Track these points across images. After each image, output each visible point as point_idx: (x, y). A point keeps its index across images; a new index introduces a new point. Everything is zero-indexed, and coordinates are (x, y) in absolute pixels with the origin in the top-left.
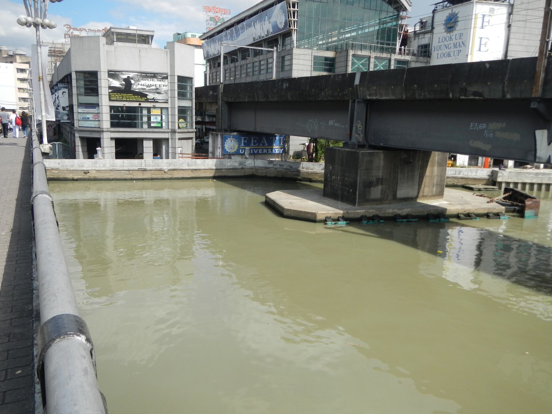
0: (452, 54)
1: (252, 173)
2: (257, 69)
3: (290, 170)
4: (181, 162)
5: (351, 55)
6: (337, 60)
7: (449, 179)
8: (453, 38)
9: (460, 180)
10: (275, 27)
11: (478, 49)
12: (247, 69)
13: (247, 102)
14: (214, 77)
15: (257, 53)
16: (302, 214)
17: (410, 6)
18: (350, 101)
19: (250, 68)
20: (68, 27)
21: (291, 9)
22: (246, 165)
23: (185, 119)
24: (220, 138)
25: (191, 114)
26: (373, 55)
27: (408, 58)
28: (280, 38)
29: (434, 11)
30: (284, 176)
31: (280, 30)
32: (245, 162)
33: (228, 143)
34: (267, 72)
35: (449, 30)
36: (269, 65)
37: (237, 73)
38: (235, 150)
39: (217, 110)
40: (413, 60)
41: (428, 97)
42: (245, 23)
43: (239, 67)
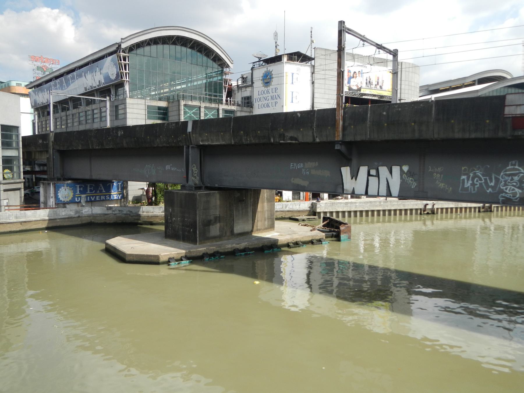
0: (270, 105)
1: (89, 221)
2: (90, 117)
3: (130, 215)
4: (7, 215)
5: (183, 105)
6: (170, 110)
7: (278, 212)
8: (270, 91)
9: (287, 213)
10: (107, 78)
12: (79, 118)
13: (81, 150)
14: (44, 126)
15: (89, 103)
16: (145, 258)
17: (232, 63)
18: (185, 147)
19: (82, 117)
21: (122, 61)
22: (82, 213)
23: (11, 169)
24: (52, 187)
25: (17, 164)
26: (203, 105)
27: (233, 108)
28: (112, 88)
29: (252, 69)
30: (124, 221)
31: (112, 81)
32: (82, 210)
33: (62, 192)
34: (101, 121)
35: (266, 85)
36: (102, 114)
37: (69, 121)
38: (70, 198)
39: (48, 159)
40: (238, 110)
41: (253, 142)
42: (75, 73)
43: (71, 116)
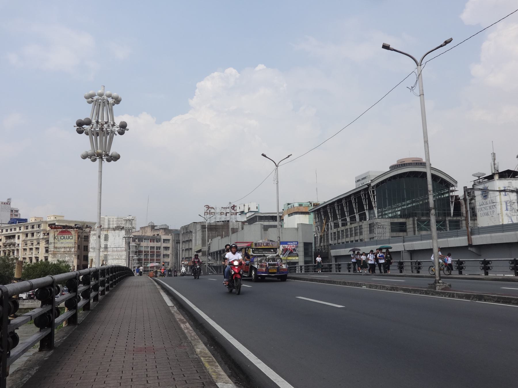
0: (489, 213)
11: (505, 209)
20: (208, 207)
